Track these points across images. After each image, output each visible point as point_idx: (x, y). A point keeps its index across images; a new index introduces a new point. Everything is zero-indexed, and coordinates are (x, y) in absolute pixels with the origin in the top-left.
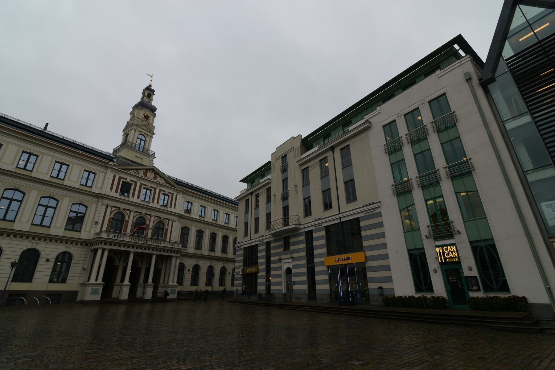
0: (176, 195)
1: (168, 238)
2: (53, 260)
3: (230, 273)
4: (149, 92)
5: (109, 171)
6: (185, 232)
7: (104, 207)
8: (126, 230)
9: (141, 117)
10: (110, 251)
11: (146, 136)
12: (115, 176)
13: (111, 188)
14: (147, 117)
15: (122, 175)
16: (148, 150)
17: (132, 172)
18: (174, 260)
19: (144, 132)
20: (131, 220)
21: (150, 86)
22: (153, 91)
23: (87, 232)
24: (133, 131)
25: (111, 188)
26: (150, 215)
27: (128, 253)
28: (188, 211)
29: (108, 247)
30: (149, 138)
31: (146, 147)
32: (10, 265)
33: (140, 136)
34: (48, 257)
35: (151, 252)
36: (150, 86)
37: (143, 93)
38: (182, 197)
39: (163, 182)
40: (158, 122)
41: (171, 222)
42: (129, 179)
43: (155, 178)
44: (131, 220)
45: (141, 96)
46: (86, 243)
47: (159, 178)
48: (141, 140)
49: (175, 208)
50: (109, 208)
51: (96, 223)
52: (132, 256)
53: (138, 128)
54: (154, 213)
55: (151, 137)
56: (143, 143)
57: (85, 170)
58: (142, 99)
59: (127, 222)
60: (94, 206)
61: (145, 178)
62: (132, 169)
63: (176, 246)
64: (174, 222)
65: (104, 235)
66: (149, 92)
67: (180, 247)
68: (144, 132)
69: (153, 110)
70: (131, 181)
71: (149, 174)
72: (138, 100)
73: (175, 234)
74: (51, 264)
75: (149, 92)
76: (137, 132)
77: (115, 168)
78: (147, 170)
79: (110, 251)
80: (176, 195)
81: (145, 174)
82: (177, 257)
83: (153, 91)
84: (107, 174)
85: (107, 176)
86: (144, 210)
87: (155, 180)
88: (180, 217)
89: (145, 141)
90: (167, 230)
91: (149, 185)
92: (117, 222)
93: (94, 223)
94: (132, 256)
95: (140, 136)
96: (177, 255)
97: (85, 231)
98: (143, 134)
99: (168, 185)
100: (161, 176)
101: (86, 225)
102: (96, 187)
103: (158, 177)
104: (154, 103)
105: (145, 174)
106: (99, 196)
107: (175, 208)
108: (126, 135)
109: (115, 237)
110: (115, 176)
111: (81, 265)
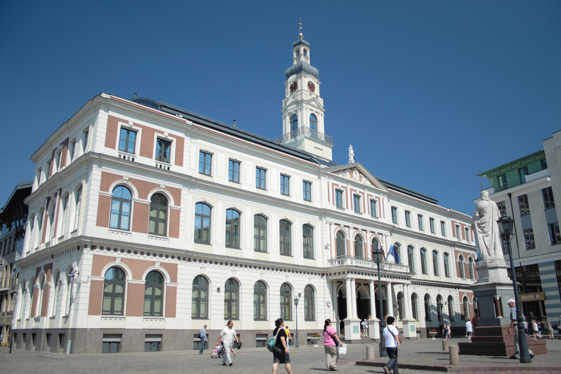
3: (446, 303)
7: (328, 225)
8: (366, 254)
11: (316, 114)
12: (328, 182)
13: (329, 201)
25: (329, 201)
39: (368, 183)
41: (384, 237)
46: (323, 273)
52: (372, 286)
54: (369, 229)
61: (352, 180)
71: (354, 174)
81: (352, 176)
84: (323, 181)
85: (323, 185)
94: (372, 286)
100: (365, 176)
103: (363, 177)
106: (322, 213)
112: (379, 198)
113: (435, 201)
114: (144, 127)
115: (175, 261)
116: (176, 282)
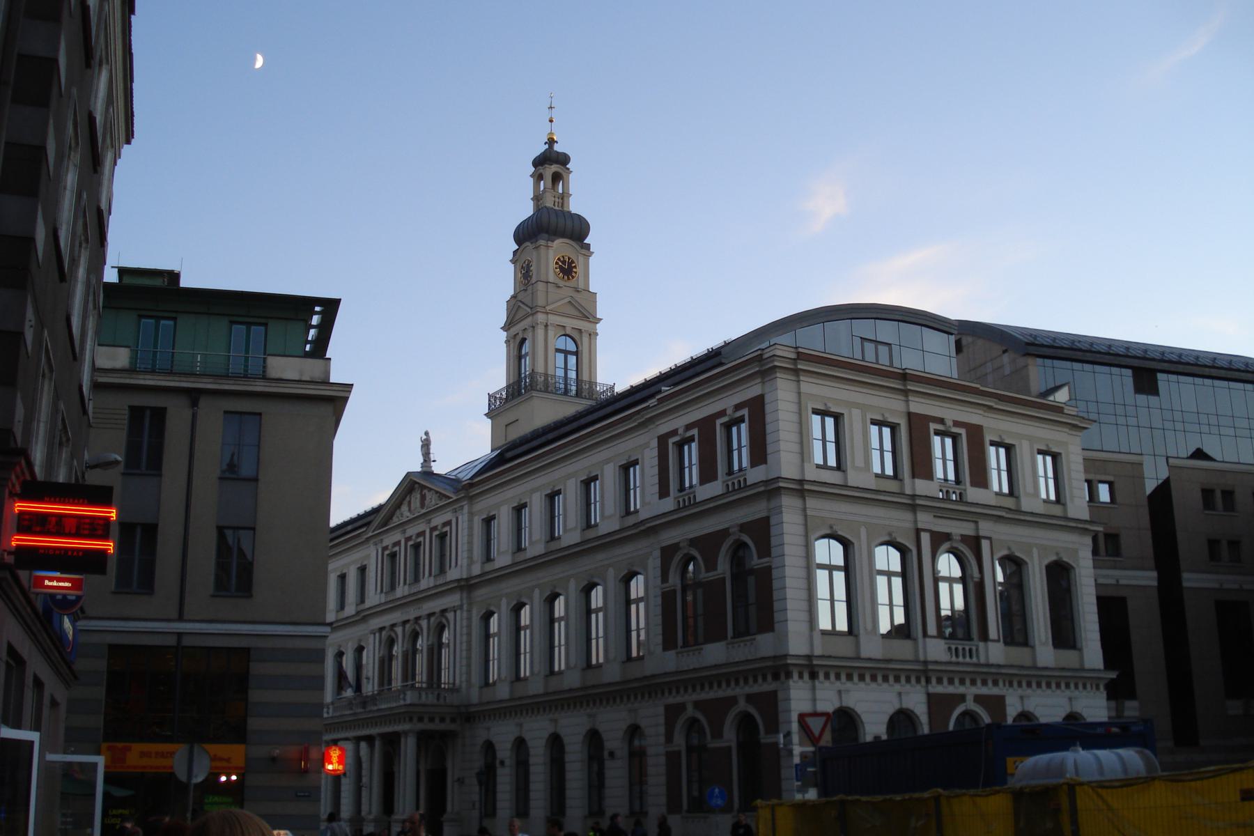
4: (551, 164)
9: (552, 278)
14: (567, 269)
16: (592, 384)
19: (570, 323)
21: (551, 142)
22: (563, 160)
24: (540, 332)
30: (585, 339)
31: (585, 377)
33: (563, 343)
36: (551, 142)
37: (538, 177)
40: (603, 272)
45: (526, 187)
48: (566, 353)
53: (553, 319)
55: (593, 335)
56: (572, 360)
58: (537, 198)
66: (551, 164)
68: (570, 323)
69: (577, 230)
72: (526, 210)
75: (555, 168)
76: (551, 333)
83: (563, 160)
89: (576, 353)
95: (563, 343)
104: (575, 206)
108: (517, 346)
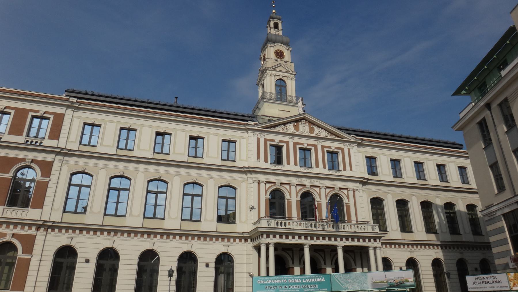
0: (349, 150)
1: (353, 218)
2: (213, 265)
5: (251, 133)
6: (377, 204)
10: (277, 246)
11: (284, 79)
12: (259, 140)
13: (259, 157)
15: (268, 136)
17: (279, 129)
18: (371, 252)
20: (293, 198)
23: (245, 223)
25: (259, 157)
26: (319, 187)
27: (301, 247)
28: (372, 169)
29: (273, 241)
32: (167, 273)
34: (207, 261)
35: (332, 242)
38: (359, 152)
39: (324, 134)
41: (351, 193)
42: (277, 139)
43: (311, 130)
44: (293, 198)
46: (244, 238)
47: (317, 130)
49: (351, 170)
50: (262, 185)
51: (252, 208)
54: (324, 183)
57: (223, 141)
59: (290, 202)
60: (244, 185)
61: (298, 133)
62: (277, 125)
63: (369, 229)
64: (356, 193)
65: (264, 224)
67: (377, 230)
70: (280, 141)
73: (363, 212)
74: (212, 270)
77: (256, 128)
78: (297, 121)
79: (277, 246)
80: (349, 150)
81: (297, 128)
82: (375, 248)
86: (309, 180)
87: (313, 133)
88: (364, 182)
90: (348, 206)
91: (306, 143)
92: (276, 204)
93: (249, 210)
96: (375, 244)
97: (240, 222)
98: (281, 77)
99: (333, 137)
100: (319, 126)
101: (240, 213)
102: (240, 160)
103: (315, 127)
105: (297, 128)
106: (247, 171)
107: (351, 170)
109: (277, 225)
110: (259, 140)
111: (245, 270)
112: (342, 149)
113: (459, 146)
114: (17, 110)
115: (33, 232)
116: (32, 254)
